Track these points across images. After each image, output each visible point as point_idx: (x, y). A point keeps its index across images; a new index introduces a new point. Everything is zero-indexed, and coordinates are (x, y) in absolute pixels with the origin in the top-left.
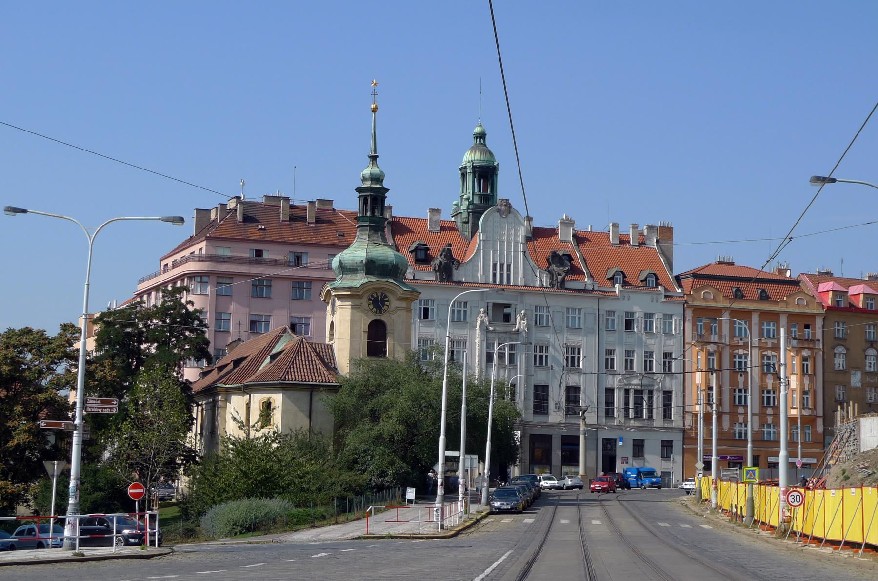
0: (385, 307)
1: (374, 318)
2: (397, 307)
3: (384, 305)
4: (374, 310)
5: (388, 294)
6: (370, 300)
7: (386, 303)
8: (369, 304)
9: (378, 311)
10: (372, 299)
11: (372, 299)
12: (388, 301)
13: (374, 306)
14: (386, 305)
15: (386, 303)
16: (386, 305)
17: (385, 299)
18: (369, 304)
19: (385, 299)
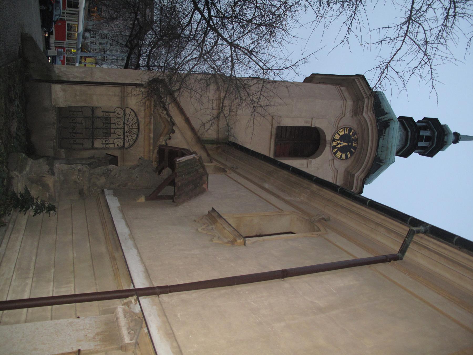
0: (339, 154)
1: (328, 138)
2: (337, 171)
5: (353, 158)
6: (350, 130)
10: (351, 134)
11: (351, 134)
15: (344, 155)
16: (341, 155)
17: (348, 153)
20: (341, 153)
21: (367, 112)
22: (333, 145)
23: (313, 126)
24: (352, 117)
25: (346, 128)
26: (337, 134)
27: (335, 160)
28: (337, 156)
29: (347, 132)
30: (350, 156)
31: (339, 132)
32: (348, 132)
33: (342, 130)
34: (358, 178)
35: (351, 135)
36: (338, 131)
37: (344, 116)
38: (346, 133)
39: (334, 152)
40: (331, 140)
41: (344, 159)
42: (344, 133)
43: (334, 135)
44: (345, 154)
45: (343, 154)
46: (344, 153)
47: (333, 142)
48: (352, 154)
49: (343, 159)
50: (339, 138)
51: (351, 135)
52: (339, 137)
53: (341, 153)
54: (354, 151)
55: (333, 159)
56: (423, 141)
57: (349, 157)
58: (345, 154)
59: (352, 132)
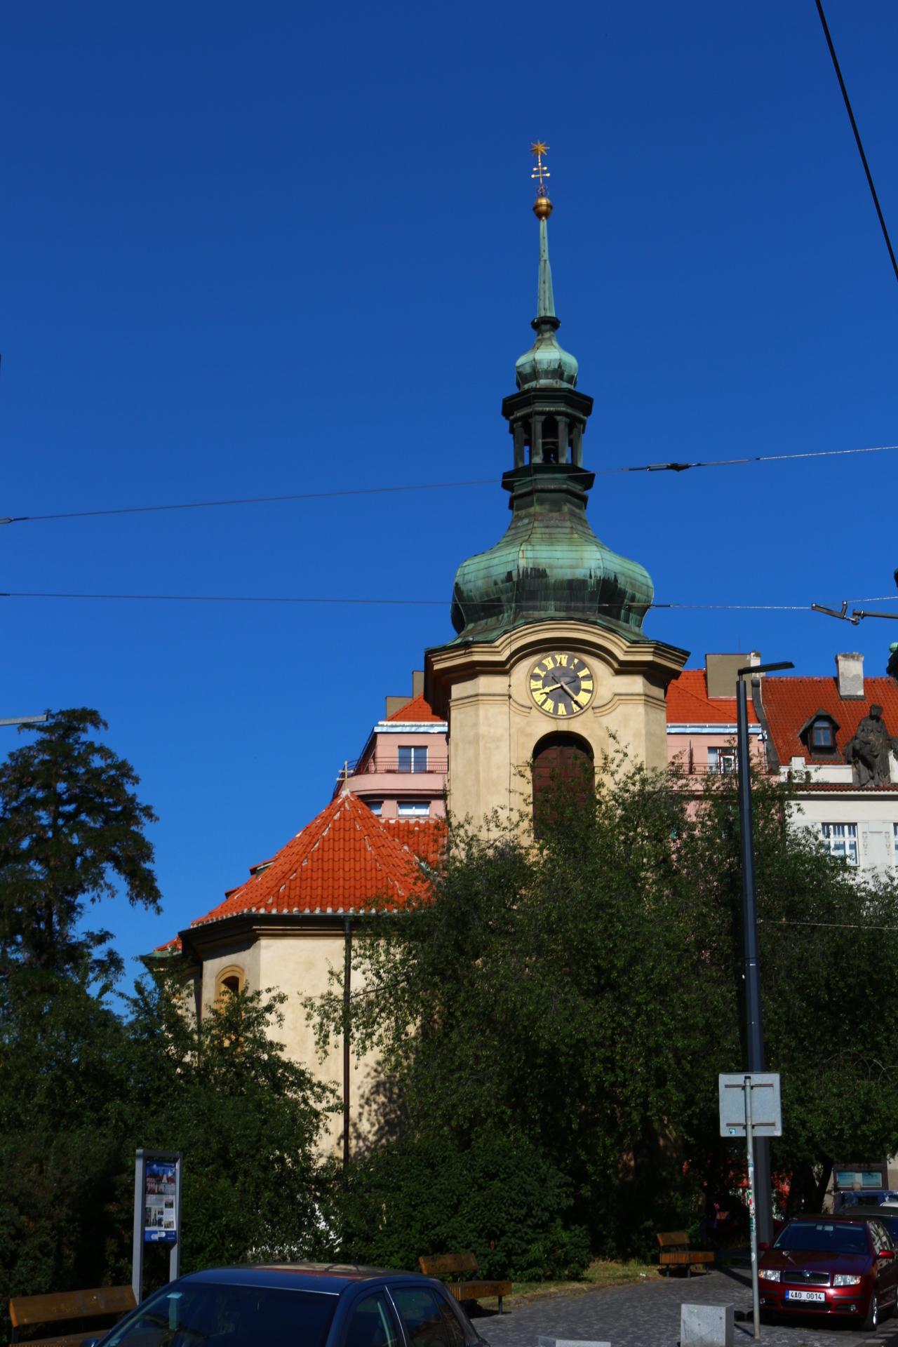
0: (583, 698)
2: (616, 695)
6: (535, 677)
7: (586, 685)
8: (533, 690)
9: (562, 709)
11: (543, 674)
12: (589, 677)
15: (586, 685)
18: (533, 690)
22: (565, 713)
25: (532, 688)
26: (543, 707)
27: (594, 705)
30: (586, 669)
31: (540, 703)
32: (539, 680)
34: (626, 652)
43: (546, 714)
45: (582, 688)
47: (560, 713)
48: (583, 665)
53: (581, 692)
55: (593, 708)
56: (557, 442)
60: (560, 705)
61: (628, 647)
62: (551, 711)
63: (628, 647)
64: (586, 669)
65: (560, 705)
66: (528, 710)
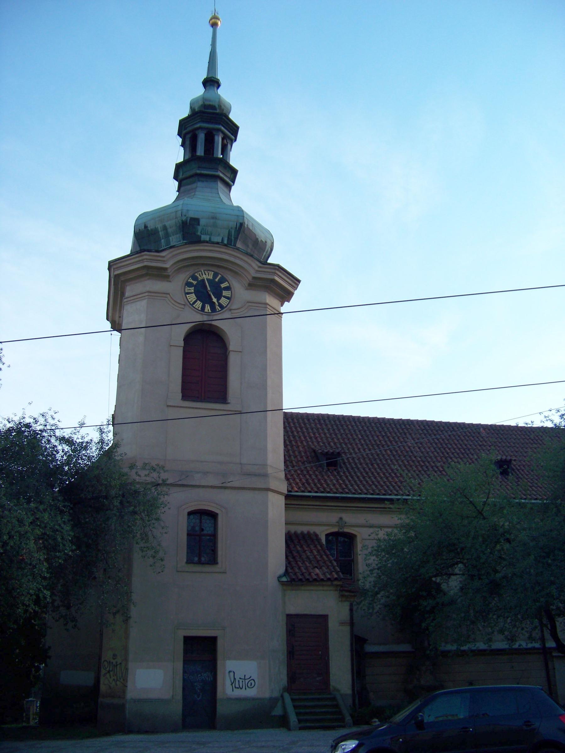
0: (223, 301)
1: (199, 318)
3: (219, 297)
4: (199, 304)
5: (229, 277)
6: (189, 284)
7: (225, 293)
8: (188, 293)
9: (208, 308)
10: (195, 283)
11: (195, 283)
12: (228, 288)
13: (199, 298)
14: (225, 297)
15: (225, 293)
16: (225, 297)
17: (223, 286)
19: (223, 286)
20: (223, 298)
21: (164, 261)
22: (210, 311)
23: (183, 345)
24: (170, 281)
25: (186, 291)
26: (194, 306)
27: (233, 307)
28: (226, 304)
29: (191, 289)
30: (227, 283)
31: (191, 303)
33: (188, 298)
35: (196, 282)
36: (190, 304)
37: (169, 294)
38: (193, 291)
39: (220, 309)
40: (203, 314)
41: (230, 292)
42: (194, 294)
44: (223, 291)
46: (222, 293)
47: (206, 310)
48: (223, 280)
49: (230, 294)
50: (200, 302)
51: (196, 282)
52: (198, 301)
53: (223, 298)
54: (220, 276)
55: (230, 310)
57: (228, 285)
58: (223, 291)
59: (192, 281)
60: (206, 305)
61: (257, 271)
62: (200, 309)
63: (257, 271)
64: (227, 283)
65: (206, 305)
66: (183, 306)
